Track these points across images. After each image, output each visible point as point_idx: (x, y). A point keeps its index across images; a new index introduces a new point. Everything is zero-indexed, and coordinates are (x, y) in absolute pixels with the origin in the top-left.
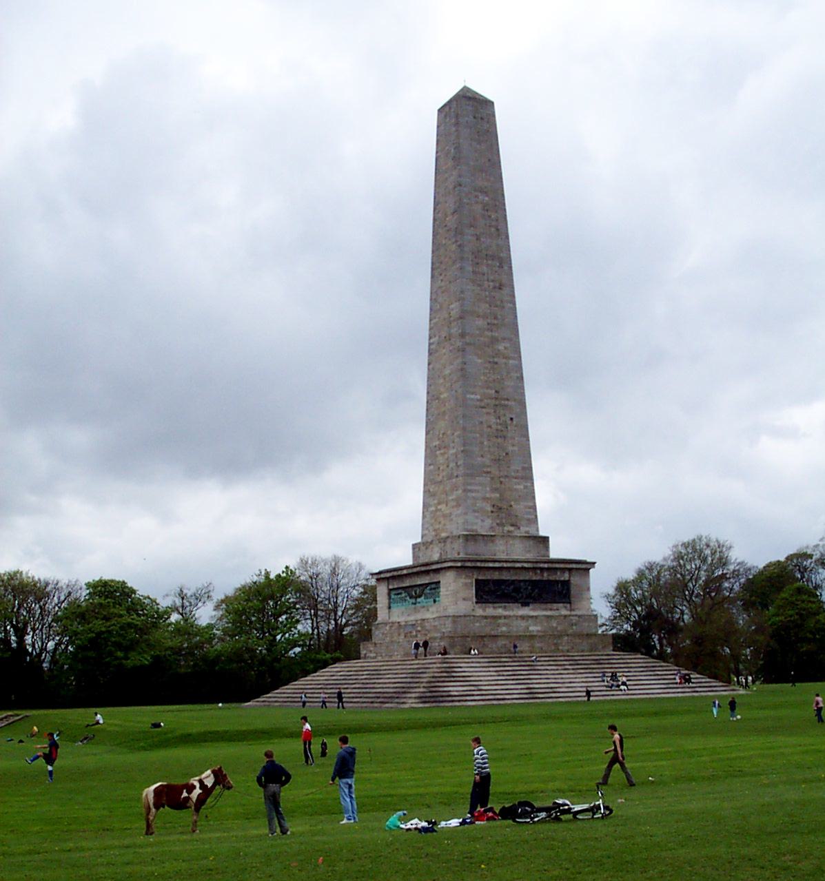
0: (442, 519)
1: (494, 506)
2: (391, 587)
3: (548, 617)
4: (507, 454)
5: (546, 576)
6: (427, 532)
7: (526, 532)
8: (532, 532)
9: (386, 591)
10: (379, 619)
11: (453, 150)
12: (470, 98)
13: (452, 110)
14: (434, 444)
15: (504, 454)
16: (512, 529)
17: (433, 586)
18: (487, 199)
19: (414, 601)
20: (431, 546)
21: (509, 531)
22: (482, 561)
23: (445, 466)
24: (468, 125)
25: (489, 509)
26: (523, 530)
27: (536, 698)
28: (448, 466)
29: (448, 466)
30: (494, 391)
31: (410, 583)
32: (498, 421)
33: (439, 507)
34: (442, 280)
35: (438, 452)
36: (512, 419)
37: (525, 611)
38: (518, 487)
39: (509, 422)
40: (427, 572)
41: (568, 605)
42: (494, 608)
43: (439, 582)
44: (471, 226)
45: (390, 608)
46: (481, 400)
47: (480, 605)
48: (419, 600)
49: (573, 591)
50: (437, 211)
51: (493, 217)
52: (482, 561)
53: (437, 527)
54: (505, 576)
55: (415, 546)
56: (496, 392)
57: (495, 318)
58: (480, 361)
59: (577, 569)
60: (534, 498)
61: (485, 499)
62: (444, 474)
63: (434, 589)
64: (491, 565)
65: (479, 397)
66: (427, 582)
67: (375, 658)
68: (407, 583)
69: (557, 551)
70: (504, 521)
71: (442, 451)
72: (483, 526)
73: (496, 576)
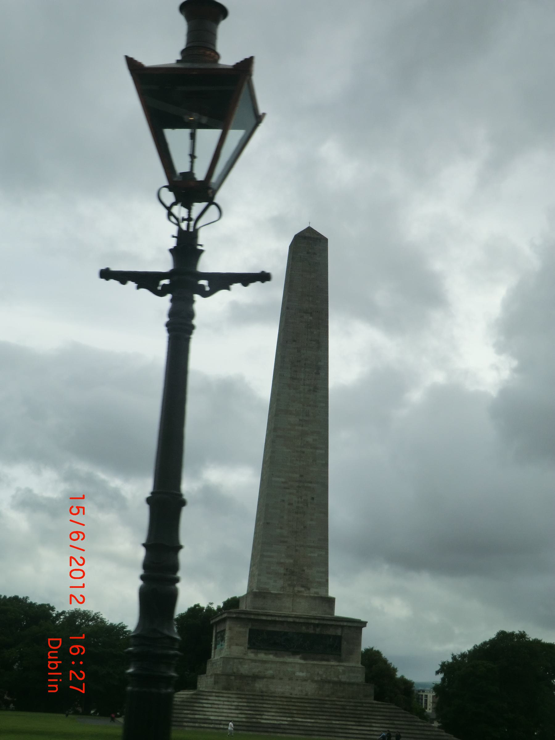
1: (287, 569)
4: (305, 527)
5: (318, 630)
7: (316, 593)
8: (322, 594)
15: (302, 527)
18: (311, 318)
21: (299, 592)
25: (282, 571)
26: (313, 591)
30: (297, 476)
32: (300, 499)
36: (313, 499)
38: (312, 555)
42: (265, 654)
44: (294, 341)
47: (252, 650)
51: (315, 332)
54: (277, 628)
56: (301, 476)
61: (280, 564)
65: (283, 480)
69: (341, 610)
70: (295, 583)
72: (274, 586)
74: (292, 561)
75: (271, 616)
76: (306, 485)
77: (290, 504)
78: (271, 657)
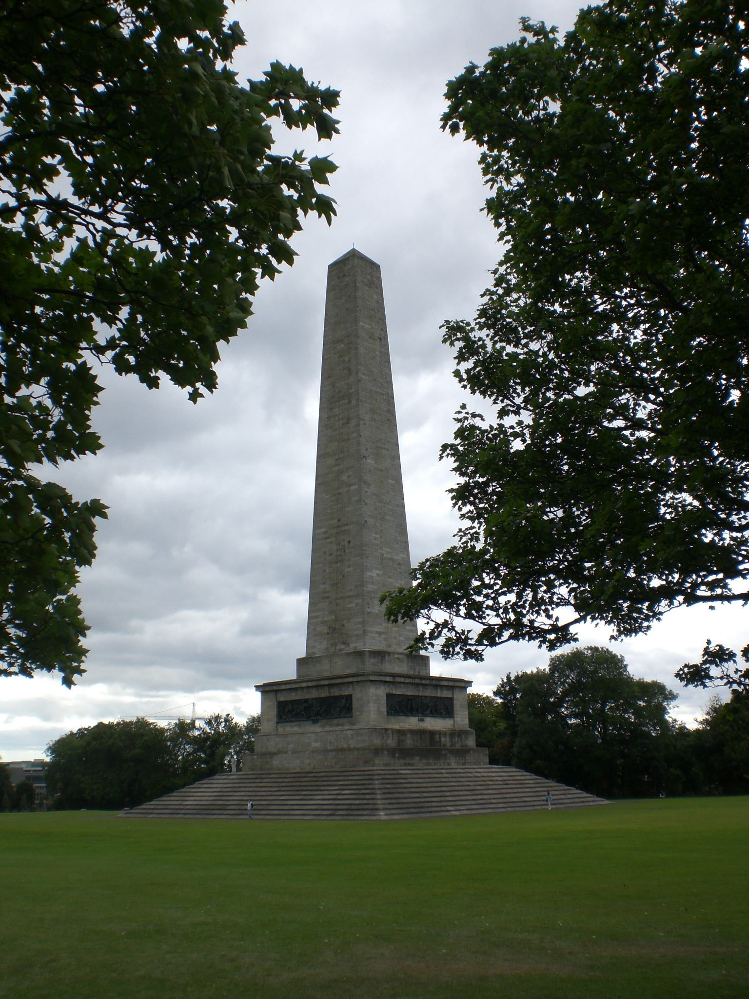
16: (343, 647)
18: (343, 345)
21: (340, 650)
25: (326, 630)
27: (431, 812)
38: (350, 605)
42: (291, 726)
46: (325, 532)
49: (355, 704)
56: (339, 520)
59: (358, 682)
61: (324, 622)
65: (324, 530)
73: (293, 696)
74: (333, 617)
76: (343, 528)
77: (331, 554)
78: (296, 729)
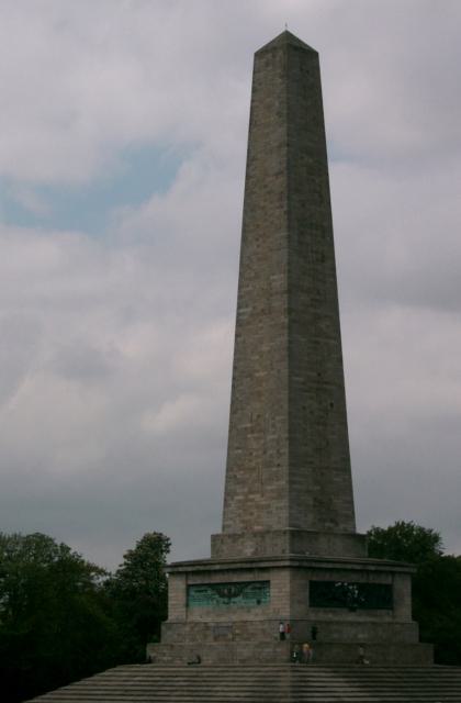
0: (255, 511)
2: (190, 582)
3: (373, 623)
4: (328, 443)
6: (231, 522)
9: (184, 587)
10: (170, 618)
11: (277, 104)
12: (296, 48)
13: (278, 59)
14: (244, 426)
16: (332, 525)
17: (258, 585)
19: (226, 600)
20: (241, 540)
21: (330, 528)
22: (316, 561)
23: (260, 452)
24: (289, 74)
25: (311, 503)
28: (265, 453)
29: (265, 453)
30: (315, 374)
31: (222, 578)
33: (251, 496)
34: (258, 246)
35: (249, 436)
37: (351, 617)
39: (329, 408)
40: (250, 570)
41: (390, 612)
43: (268, 582)
45: (187, 605)
46: (304, 383)
48: (233, 600)
50: (251, 168)
52: (316, 561)
53: (247, 518)
55: (214, 538)
56: (319, 375)
57: (319, 293)
58: (303, 340)
60: (351, 491)
62: (260, 460)
63: (260, 588)
64: (324, 565)
65: (301, 379)
66: (248, 580)
67: (171, 661)
68: (217, 579)
71: (255, 435)
73: (327, 577)
75: (328, 562)
78: (330, 616)
